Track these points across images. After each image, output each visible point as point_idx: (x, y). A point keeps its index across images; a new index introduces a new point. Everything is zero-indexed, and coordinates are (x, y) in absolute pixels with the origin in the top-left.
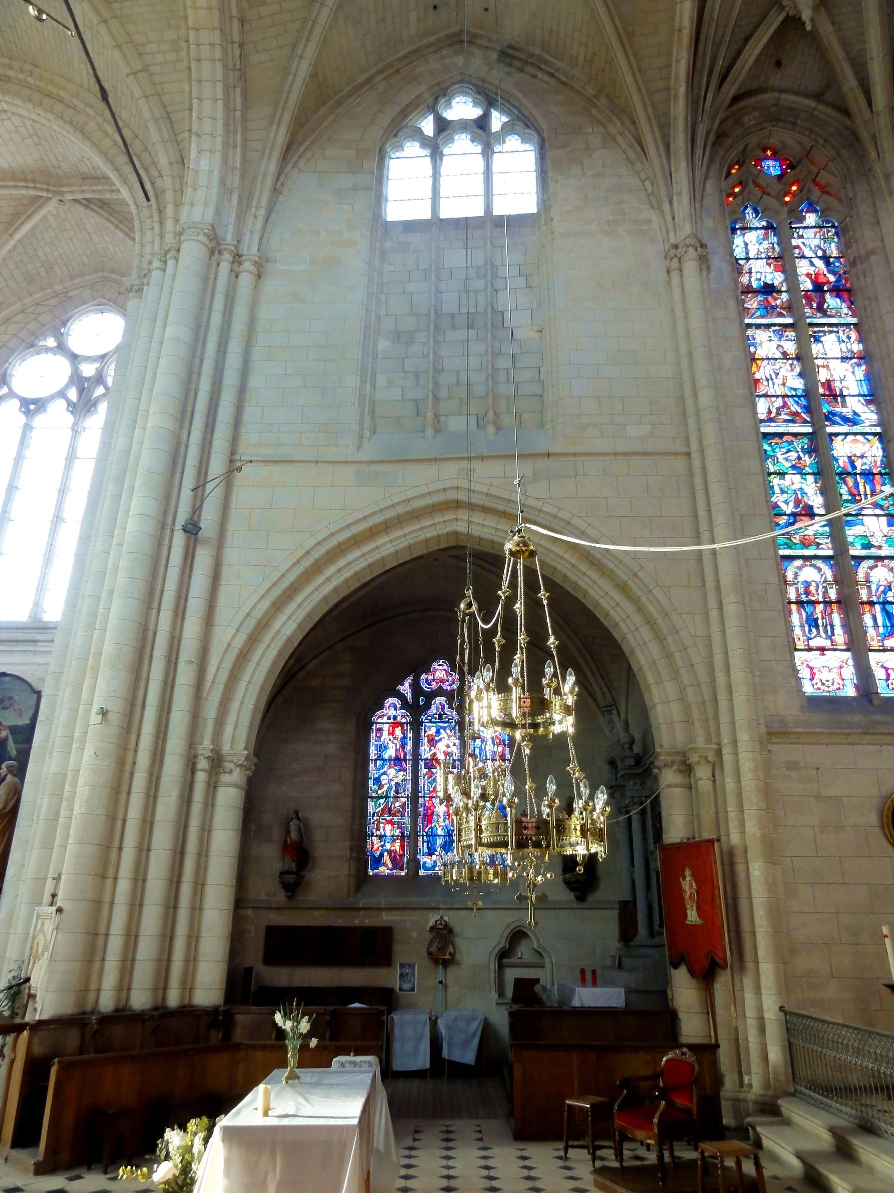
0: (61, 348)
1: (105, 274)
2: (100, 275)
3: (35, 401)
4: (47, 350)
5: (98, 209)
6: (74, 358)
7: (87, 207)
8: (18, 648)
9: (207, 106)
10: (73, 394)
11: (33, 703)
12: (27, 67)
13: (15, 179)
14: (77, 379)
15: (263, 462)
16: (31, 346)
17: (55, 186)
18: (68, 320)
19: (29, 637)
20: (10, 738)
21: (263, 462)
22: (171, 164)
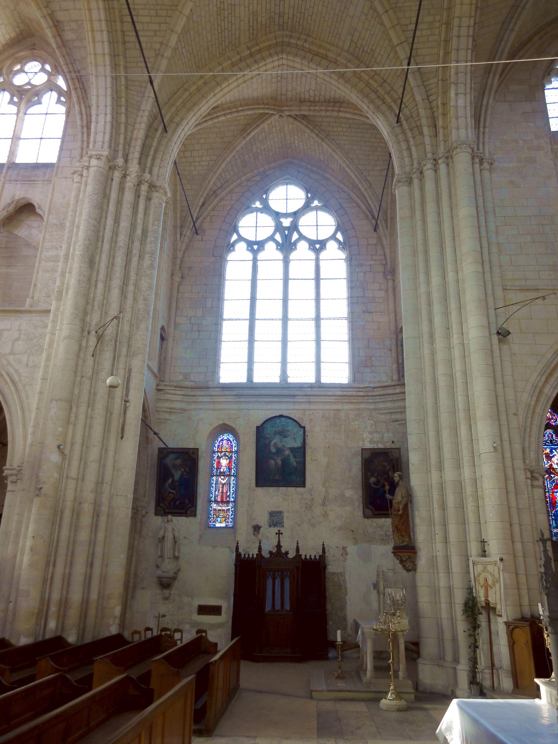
0: (267, 209)
1: (290, 160)
2: (286, 160)
3: (256, 243)
4: (257, 210)
5: (301, 120)
6: (277, 215)
7: (295, 119)
8: (284, 400)
10: (278, 237)
11: (301, 433)
12: (303, 37)
13: (258, 104)
14: (279, 228)
16: (248, 209)
17: (279, 106)
18: (268, 190)
19: (291, 393)
20: (291, 454)
22: (423, 100)
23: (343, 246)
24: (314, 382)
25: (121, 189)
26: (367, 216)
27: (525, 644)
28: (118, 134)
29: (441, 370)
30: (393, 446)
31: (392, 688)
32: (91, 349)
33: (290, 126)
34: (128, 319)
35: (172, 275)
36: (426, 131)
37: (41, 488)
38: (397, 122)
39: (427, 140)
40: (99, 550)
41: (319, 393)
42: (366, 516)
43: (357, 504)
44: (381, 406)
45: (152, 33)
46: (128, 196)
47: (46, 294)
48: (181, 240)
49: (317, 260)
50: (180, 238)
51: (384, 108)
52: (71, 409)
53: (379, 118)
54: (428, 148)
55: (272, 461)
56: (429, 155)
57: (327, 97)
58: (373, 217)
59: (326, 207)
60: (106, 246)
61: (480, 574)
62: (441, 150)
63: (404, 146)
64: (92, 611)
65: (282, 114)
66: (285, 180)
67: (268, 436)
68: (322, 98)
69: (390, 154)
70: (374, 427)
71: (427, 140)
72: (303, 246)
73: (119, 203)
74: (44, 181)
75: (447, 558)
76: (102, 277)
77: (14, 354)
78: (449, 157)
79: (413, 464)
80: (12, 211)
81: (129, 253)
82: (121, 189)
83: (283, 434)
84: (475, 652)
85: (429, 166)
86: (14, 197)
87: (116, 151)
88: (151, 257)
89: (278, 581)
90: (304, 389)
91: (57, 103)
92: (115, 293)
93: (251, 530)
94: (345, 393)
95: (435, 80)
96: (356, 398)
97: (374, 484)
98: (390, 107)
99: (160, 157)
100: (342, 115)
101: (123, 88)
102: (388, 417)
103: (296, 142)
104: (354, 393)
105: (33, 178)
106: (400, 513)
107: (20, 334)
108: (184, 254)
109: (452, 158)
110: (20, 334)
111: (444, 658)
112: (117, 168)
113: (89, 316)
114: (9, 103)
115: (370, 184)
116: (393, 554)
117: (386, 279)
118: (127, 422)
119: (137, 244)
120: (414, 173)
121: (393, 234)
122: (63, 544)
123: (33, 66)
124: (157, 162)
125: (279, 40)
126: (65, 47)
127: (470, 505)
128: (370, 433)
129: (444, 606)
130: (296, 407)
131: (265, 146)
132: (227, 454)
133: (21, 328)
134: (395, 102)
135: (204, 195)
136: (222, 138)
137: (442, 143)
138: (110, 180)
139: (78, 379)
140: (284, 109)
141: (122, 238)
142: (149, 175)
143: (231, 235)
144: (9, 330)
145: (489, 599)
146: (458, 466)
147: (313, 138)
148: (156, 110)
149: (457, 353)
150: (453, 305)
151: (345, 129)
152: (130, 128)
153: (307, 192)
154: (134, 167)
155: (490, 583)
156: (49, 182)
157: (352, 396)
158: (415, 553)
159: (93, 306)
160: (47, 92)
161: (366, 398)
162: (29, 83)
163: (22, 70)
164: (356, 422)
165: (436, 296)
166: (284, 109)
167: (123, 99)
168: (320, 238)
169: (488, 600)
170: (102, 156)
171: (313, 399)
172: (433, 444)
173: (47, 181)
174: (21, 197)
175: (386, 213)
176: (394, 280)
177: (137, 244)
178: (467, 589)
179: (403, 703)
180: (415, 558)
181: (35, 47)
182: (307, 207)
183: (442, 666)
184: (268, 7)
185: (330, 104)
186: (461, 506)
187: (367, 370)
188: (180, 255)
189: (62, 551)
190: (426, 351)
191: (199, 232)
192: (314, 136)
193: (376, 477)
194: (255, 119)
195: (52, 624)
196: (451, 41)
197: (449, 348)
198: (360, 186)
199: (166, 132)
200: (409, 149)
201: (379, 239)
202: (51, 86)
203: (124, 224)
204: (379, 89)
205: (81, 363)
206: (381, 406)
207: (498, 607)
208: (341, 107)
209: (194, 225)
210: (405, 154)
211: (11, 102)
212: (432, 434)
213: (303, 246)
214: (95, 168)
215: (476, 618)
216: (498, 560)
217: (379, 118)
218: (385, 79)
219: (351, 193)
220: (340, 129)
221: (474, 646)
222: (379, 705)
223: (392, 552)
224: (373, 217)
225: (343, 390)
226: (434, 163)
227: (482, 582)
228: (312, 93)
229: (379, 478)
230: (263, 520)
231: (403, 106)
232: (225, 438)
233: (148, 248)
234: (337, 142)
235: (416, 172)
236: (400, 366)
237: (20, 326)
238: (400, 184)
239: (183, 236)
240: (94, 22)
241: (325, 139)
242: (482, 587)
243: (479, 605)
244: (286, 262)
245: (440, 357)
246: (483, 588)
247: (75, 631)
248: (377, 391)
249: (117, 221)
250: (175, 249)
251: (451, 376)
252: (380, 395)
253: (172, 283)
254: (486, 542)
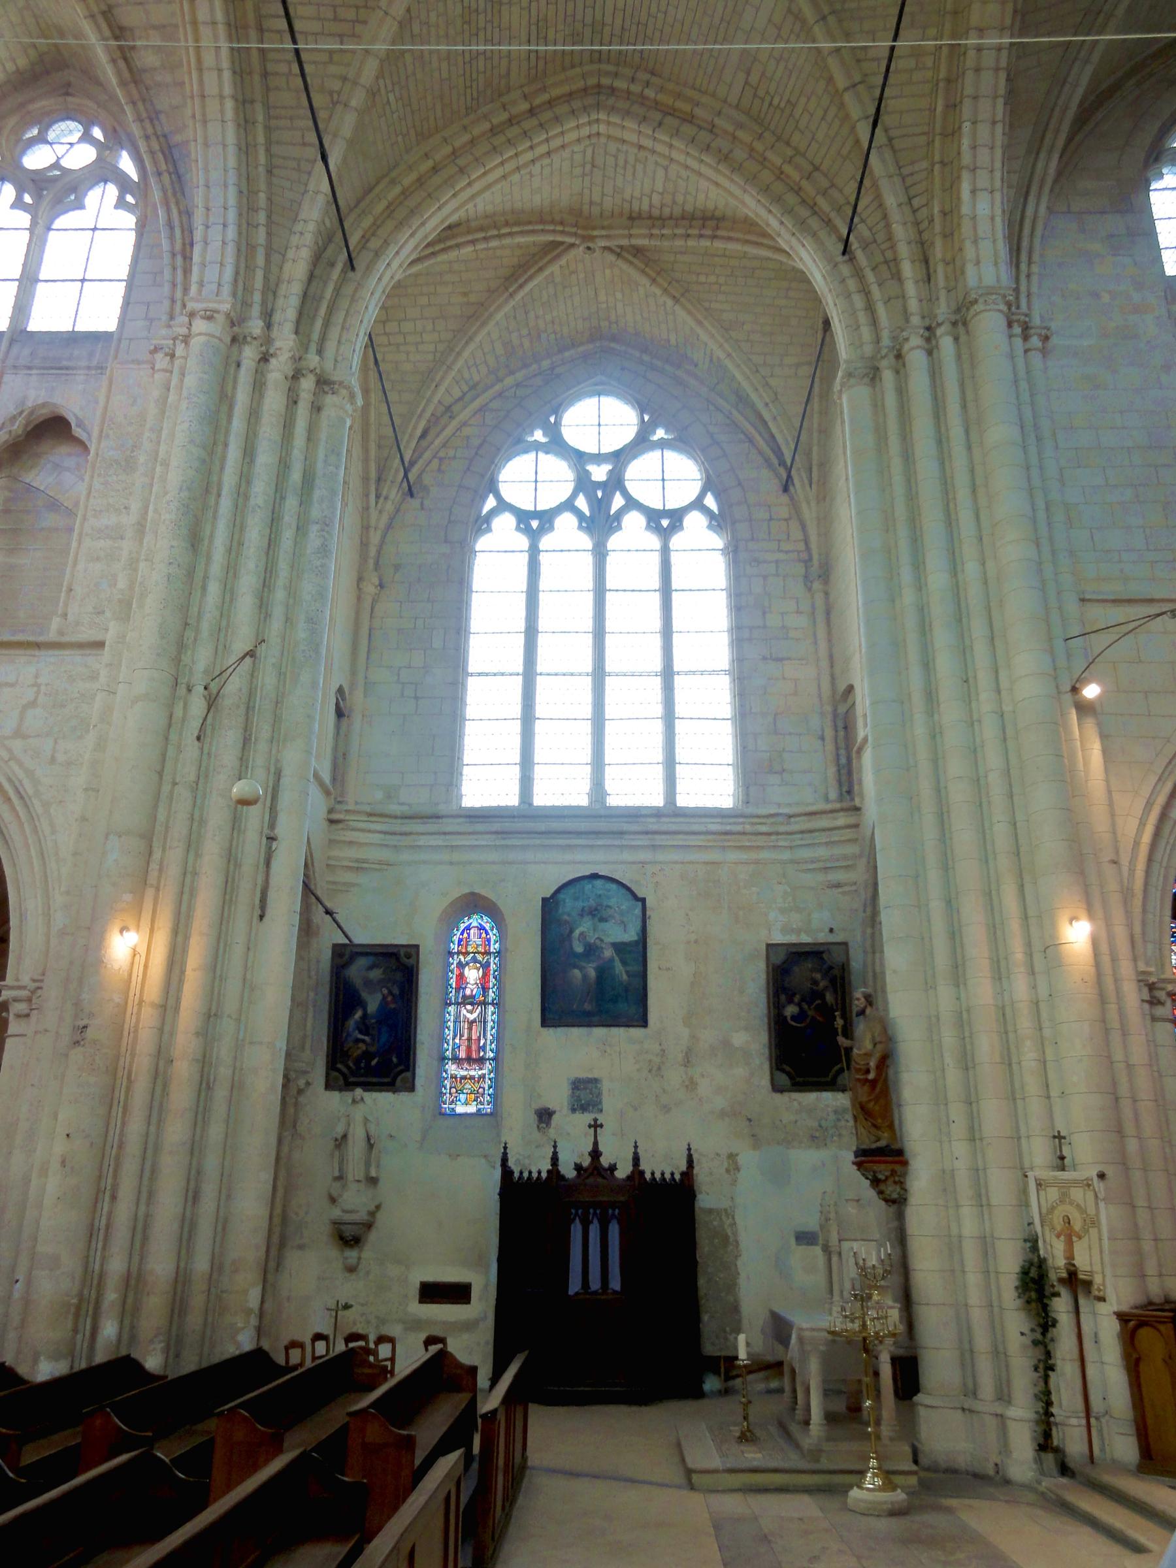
0: (557, 445)
3: (536, 514)
4: (537, 447)
5: (630, 258)
6: (579, 459)
7: (619, 255)
8: (599, 842)
9: (984, 130)
10: (582, 503)
11: (638, 911)
12: (643, 76)
13: (542, 221)
14: (583, 483)
15: (1114, 601)
17: (585, 228)
18: (560, 405)
20: (616, 958)
21: (1114, 601)
22: (900, 205)
23: (718, 522)
24: (661, 804)
25: (258, 386)
26: (767, 461)
27: (1164, 1360)
28: (250, 268)
29: (956, 767)
30: (832, 939)
31: (873, 1463)
32: (194, 725)
33: (608, 272)
34: (274, 660)
35: (360, 579)
36: (908, 269)
37: (85, 1027)
38: (844, 253)
39: (911, 289)
40: (211, 1163)
41: (674, 828)
42: (777, 1088)
43: (757, 1062)
44: (806, 854)
45: (325, 57)
46: (274, 401)
48: (379, 505)
49: (665, 552)
50: (377, 503)
51: (814, 223)
52: (150, 854)
53: (804, 246)
54: (913, 305)
55: (577, 972)
56: (915, 320)
57: (689, 208)
58: (782, 463)
59: (681, 442)
60: (226, 505)
61: (1052, 1209)
62: (943, 310)
63: (858, 301)
64: (197, 1301)
65: (591, 245)
66: (596, 385)
67: (566, 917)
68: (677, 211)
69: (827, 324)
70: (790, 898)
71: (911, 289)
72: (634, 521)
73: (254, 414)
74: (89, 368)
75: (978, 1174)
76: (216, 569)
77: (25, 737)
78: (961, 322)
79: (895, 972)
80: (20, 432)
81: (274, 521)
82: (258, 386)
83: (597, 913)
84: (1046, 1378)
85: (916, 341)
87: (246, 304)
88: (323, 530)
89: (594, 1230)
90: (643, 820)
91: (116, 207)
92: (245, 605)
93: (533, 1119)
94: (728, 828)
95: (925, 164)
96: (753, 837)
97: (793, 1018)
98: (828, 222)
99: (341, 321)
100: (719, 244)
101: (261, 169)
102: (821, 877)
103: (620, 305)
104: (748, 828)
105: (65, 363)
106: (871, 1076)
107: (38, 692)
108: (384, 536)
109: (965, 324)
110: (38, 692)
111: (975, 1394)
112: (249, 339)
113: (189, 653)
114: (13, 206)
115: (776, 394)
116: (855, 1167)
117: (810, 589)
118: (274, 881)
119: (291, 503)
120: (883, 358)
121: (824, 494)
122: (133, 1147)
123: (67, 131)
124: (334, 333)
125: (592, 81)
126: (135, 82)
127: (1029, 1056)
128: (782, 911)
129: (973, 1279)
130: (627, 856)
131: (555, 313)
132: (479, 957)
133: (39, 681)
134: (839, 210)
135: (427, 415)
136: (465, 294)
137: (943, 294)
138: (234, 365)
139: (166, 788)
140: (595, 233)
141: (260, 489)
142: (317, 358)
143: (484, 499)
144: (12, 685)
145: (1075, 1262)
146: (1000, 972)
147: (655, 295)
148: (331, 222)
149: (989, 731)
150: (978, 629)
151: (722, 280)
152: (276, 258)
153: (642, 410)
154: (285, 340)
155: (1077, 1226)
157: (744, 833)
158: (905, 1163)
159: (197, 631)
160: (97, 183)
161: (773, 837)
162: (56, 165)
163: (42, 139)
164: (754, 889)
165: (940, 610)
166: (595, 233)
167: (262, 196)
168: (670, 506)
169: (1074, 1265)
170: (218, 312)
171: (659, 840)
172: (939, 925)
173: (97, 368)
174: (40, 402)
175: (809, 454)
176: (826, 594)
177: (291, 503)
178: (1025, 1241)
179: (899, 1496)
180: (905, 1174)
181: (70, 90)
182: (641, 443)
183: (971, 1411)
184: (570, 11)
185: (694, 223)
186: (1008, 1061)
187: (774, 779)
188: (375, 538)
189: (130, 1167)
190: (920, 730)
191: (415, 491)
192: (658, 292)
193: (799, 1005)
194: (534, 255)
195: (109, 1329)
196: (960, 81)
197: (972, 722)
198: (754, 397)
199: (353, 268)
200: (870, 308)
201: (794, 505)
202: (103, 171)
203: (265, 458)
204: (804, 183)
205: (171, 752)
206: (806, 854)
207: (1098, 1280)
208: (717, 228)
209: (406, 476)
210: (862, 317)
211: (18, 204)
212: (936, 906)
213: (634, 521)
214: (202, 339)
215: (1047, 1305)
216: (1095, 1179)
217: (804, 246)
218: (817, 161)
219: (735, 412)
220: (712, 279)
221: (1046, 1367)
222: (845, 1503)
223: (854, 1163)
224: (782, 463)
225: (725, 820)
226: (927, 334)
227: (1059, 1224)
228: (656, 199)
229: (805, 1006)
230: (558, 1097)
231: (856, 220)
232: (475, 924)
233: (315, 512)
234: (706, 304)
235: (886, 356)
236: (844, 771)
238: (852, 381)
239: (381, 500)
240: (201, 28)
241: (682, 299)
242: (1058, 1236)
243: (1053, 1277)
244: (600, 554)
245: (953, 739)
246: (1062, 1238)
247: (162, 1345)
248: (796, 823)
249: (249, 453)
250: (366, 528)
251: (978, 782)
252: (802, 832)
253: (359, 598)
254: (1064, 1138)
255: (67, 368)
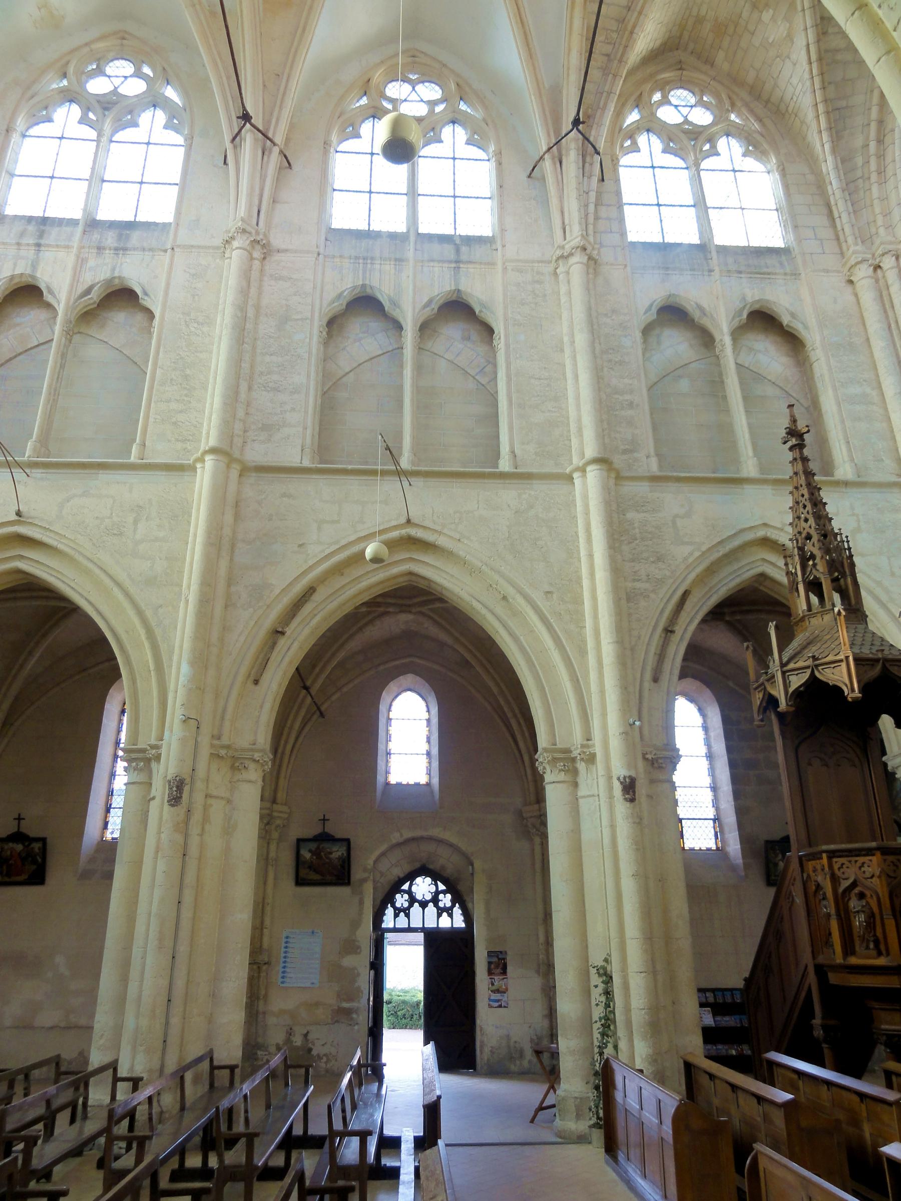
47: (874, 456)
74: (785, 274)
86: (744, 299)
105: (765, 270)
107: (858, 521)
110: (858, 521)
123: (681, 96)
156: (793, 277)
163: (665, 101)
181: (684, 66)
237: (852, 508)
255: (769, 274)
